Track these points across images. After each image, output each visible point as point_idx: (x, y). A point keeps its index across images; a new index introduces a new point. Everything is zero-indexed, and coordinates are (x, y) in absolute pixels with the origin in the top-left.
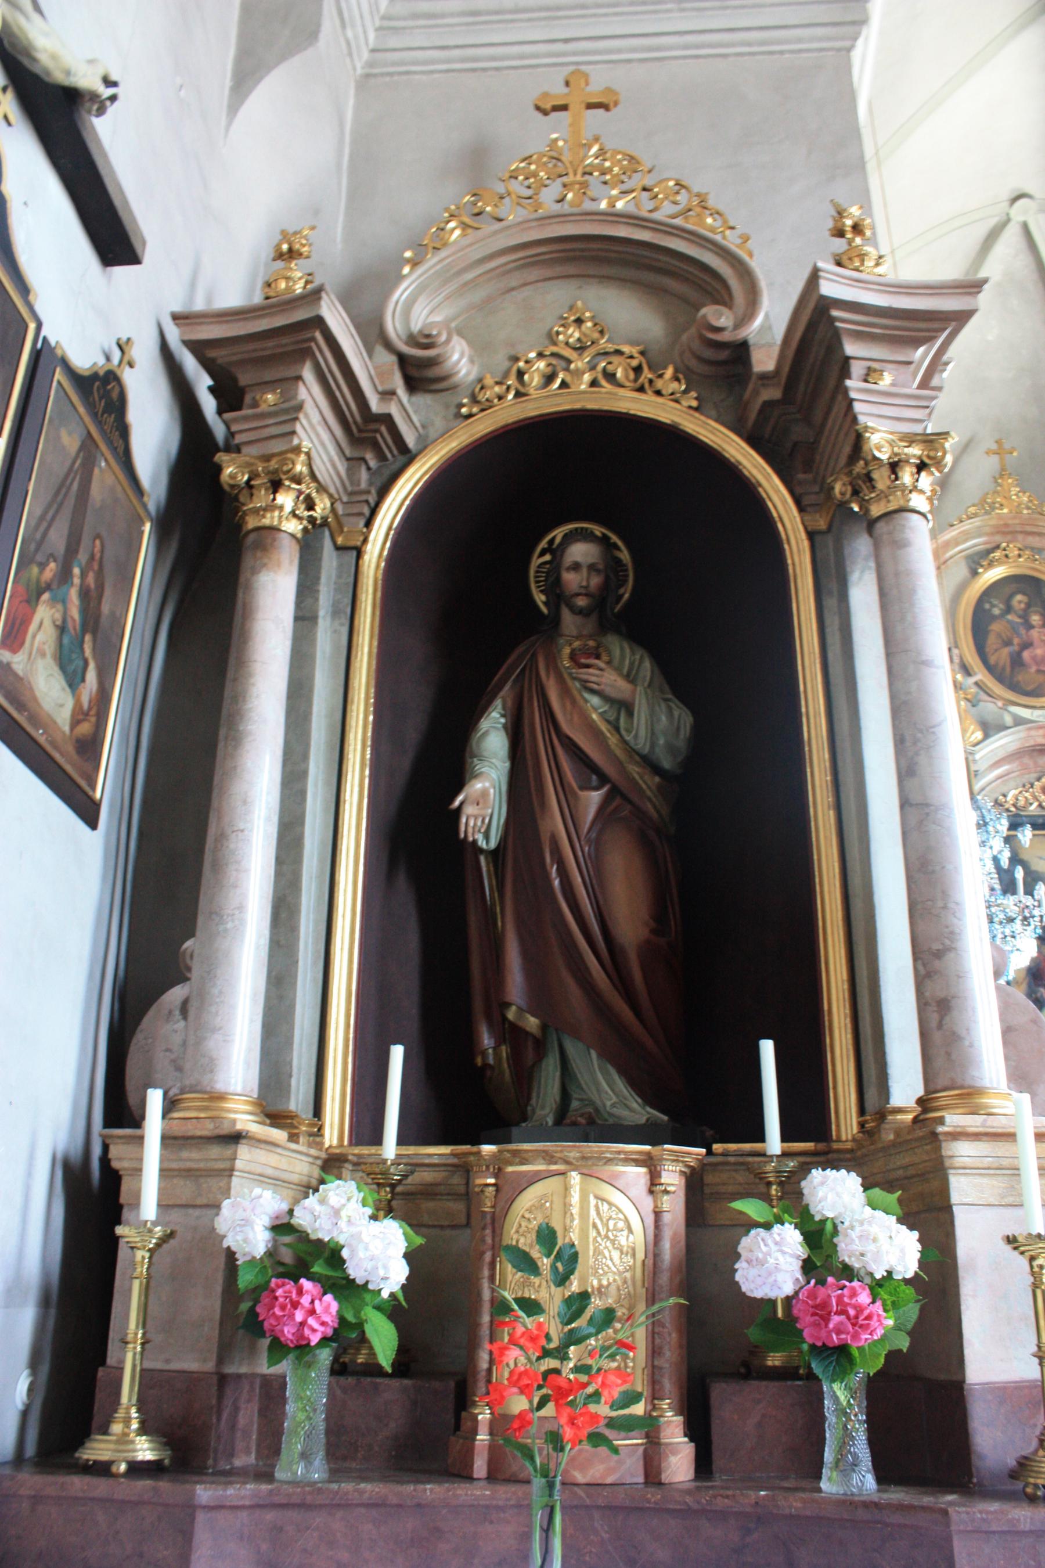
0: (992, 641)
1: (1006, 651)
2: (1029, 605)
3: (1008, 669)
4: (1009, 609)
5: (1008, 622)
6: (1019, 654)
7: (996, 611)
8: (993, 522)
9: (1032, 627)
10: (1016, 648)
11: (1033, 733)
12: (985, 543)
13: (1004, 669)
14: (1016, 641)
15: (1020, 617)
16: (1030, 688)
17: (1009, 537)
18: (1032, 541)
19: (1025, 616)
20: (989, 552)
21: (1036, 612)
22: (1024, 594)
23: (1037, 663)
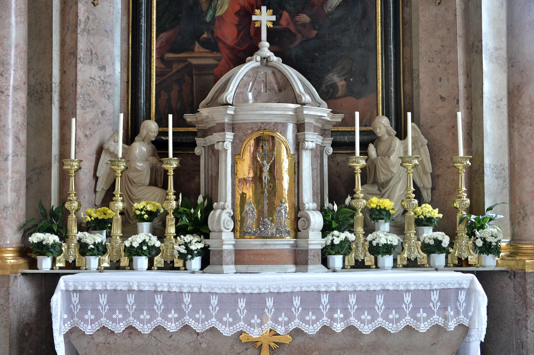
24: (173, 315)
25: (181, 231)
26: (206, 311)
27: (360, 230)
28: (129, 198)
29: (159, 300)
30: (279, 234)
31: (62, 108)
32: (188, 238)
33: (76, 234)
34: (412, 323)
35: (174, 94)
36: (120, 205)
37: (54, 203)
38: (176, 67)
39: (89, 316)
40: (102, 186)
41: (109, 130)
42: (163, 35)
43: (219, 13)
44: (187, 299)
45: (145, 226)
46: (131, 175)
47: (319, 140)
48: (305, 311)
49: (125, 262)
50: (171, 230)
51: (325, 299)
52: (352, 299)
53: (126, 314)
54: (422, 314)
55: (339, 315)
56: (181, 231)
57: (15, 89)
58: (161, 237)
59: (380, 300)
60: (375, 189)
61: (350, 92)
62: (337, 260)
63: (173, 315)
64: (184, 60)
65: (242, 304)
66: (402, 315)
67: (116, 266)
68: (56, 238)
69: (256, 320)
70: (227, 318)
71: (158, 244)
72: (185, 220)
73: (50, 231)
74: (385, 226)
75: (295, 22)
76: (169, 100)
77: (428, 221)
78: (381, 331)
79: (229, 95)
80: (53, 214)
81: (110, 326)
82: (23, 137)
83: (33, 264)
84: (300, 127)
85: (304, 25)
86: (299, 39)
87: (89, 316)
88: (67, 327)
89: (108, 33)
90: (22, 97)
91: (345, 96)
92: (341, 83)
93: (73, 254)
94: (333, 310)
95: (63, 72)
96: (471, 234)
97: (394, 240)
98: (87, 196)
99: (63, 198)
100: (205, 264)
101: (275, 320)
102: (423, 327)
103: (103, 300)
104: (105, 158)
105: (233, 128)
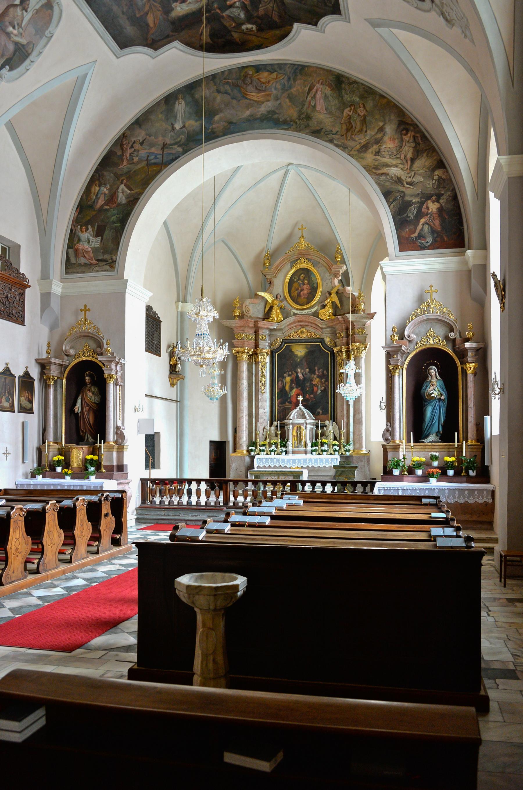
0: (293, 289)
1: (296, 292)
2: (305, 278)
3: (296, 297)
4: (299, 279)
5: (298, 283)
6: (300, 293)
7: (296, 280)
8: (298, 252)
9: (304, 284)
10: (299, 291)
11: (296, 318)
12: (296, 258)
13: (295, 298)
14: (299, 289)
15: (302, 281)
16: (301, 303)
17: (302, 256)
18: (309, 257)
19: (303, 281)
20: (297, 260)
21: (306, 280)
22: (304, 274)
23: (304, 295)
24: (278, 463)
25: (281, 447)
26: (284, 463)
27: (320, 446)
28: (270, 439)
29: (275, 460)
30: (301, 447)
31: (255, 419)
32: (282, 448)
33: (259, 447)
34: (325, 465)
35: (281, 414)
36: (268, 441)
37: (254, 440)
38: (282, 408)
39: (261, 463)
40: (264, 437)
41: (266, 424)
42: (279, 400)
43: (292, 395)
44: (280, 460)
45: (274, 446)
46: (271, 434)
47: (312, 427)
48: (304, 463)
49: (269, 453)
50: (279, 446)
51: (308, 460)
52: (313, 460)
53: (269, 463)
54: (327, 464)
55: (310, 463)
56: (281, 447)
57: (246, 416)
58: (277, 448)
59: (319, 460)
60: (326, 437)
61: (323, 414)
62: (314, 453)
63: (278, 463)
64: (284, 406)
65: (291, 461)
66: (323, 464)
67: (267, 454)
68: (255, 448)
69: (294, 464)
70: (288, 464)
71: (276, 449)
72: (282, 444)
73: (253, 446)
74: (326, 446)
75: (310, 397)
76: (280, 416)
77: (335, 445)
78: (319, 467)
79: (291, 418)
80: (254, 443)
81: (266, 465)
82: (247, 426)
83: (250, 454)
84: (306, 424)
85: (312, 397)
86: (311, 401)
87: (261, 463)
88: (257, 466)
89: (266, 401)
90: (247, 417)
91: (322, 414)
92: (321, 412)
93: (258, 451)
94: (309, 463)
95: (255, 411)
96: (333, 447)
97: (327, 449)
98: (261, 439)
99: (256, 439)
100: (286, 453)
101: (298, 464)
102: (327, 466)
103: (264, 460)
104: (265, 430)
105: (292, 424)
